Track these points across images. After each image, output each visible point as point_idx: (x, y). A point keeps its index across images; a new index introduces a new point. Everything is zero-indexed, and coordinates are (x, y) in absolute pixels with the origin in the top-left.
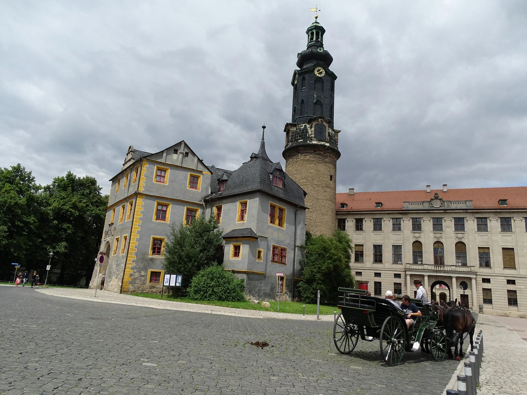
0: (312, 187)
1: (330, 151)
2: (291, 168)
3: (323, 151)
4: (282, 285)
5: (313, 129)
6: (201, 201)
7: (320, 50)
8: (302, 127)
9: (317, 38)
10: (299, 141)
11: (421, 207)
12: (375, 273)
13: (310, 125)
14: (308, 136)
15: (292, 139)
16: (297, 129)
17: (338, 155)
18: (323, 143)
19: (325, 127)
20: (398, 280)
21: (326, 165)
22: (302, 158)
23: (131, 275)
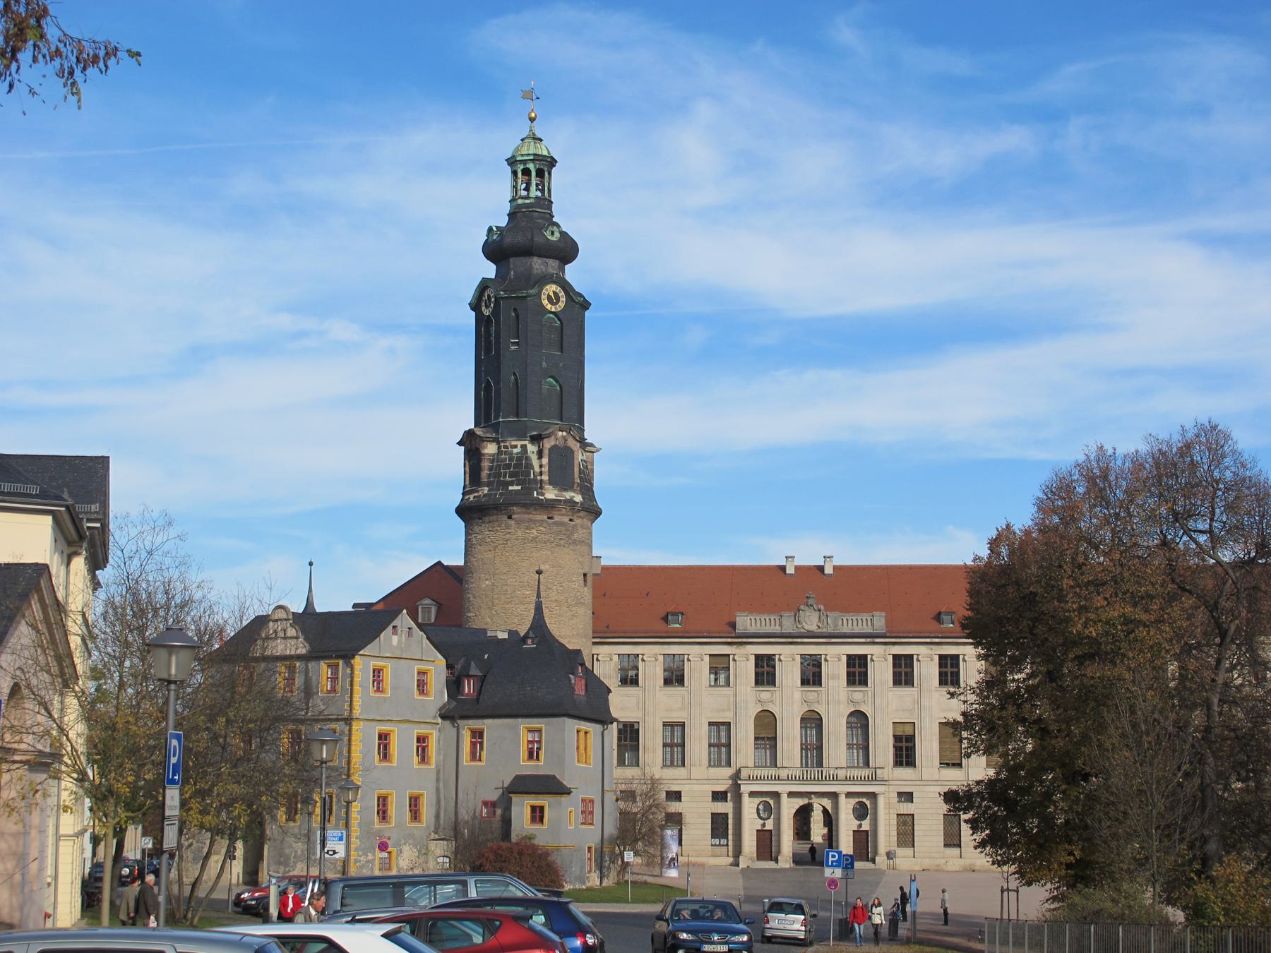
1: (582, 514)
2: (490, 555)
5: (545, 461)
8: (515, 451)
10: (511, 488)
11: (778, 628)
14: (532, 476)
15: (489, 476)
16: (500, 452)
17: (595, 513)
18: (568, 495)
20: (721, 807)
21: (574, 551)
22: (520, 533)
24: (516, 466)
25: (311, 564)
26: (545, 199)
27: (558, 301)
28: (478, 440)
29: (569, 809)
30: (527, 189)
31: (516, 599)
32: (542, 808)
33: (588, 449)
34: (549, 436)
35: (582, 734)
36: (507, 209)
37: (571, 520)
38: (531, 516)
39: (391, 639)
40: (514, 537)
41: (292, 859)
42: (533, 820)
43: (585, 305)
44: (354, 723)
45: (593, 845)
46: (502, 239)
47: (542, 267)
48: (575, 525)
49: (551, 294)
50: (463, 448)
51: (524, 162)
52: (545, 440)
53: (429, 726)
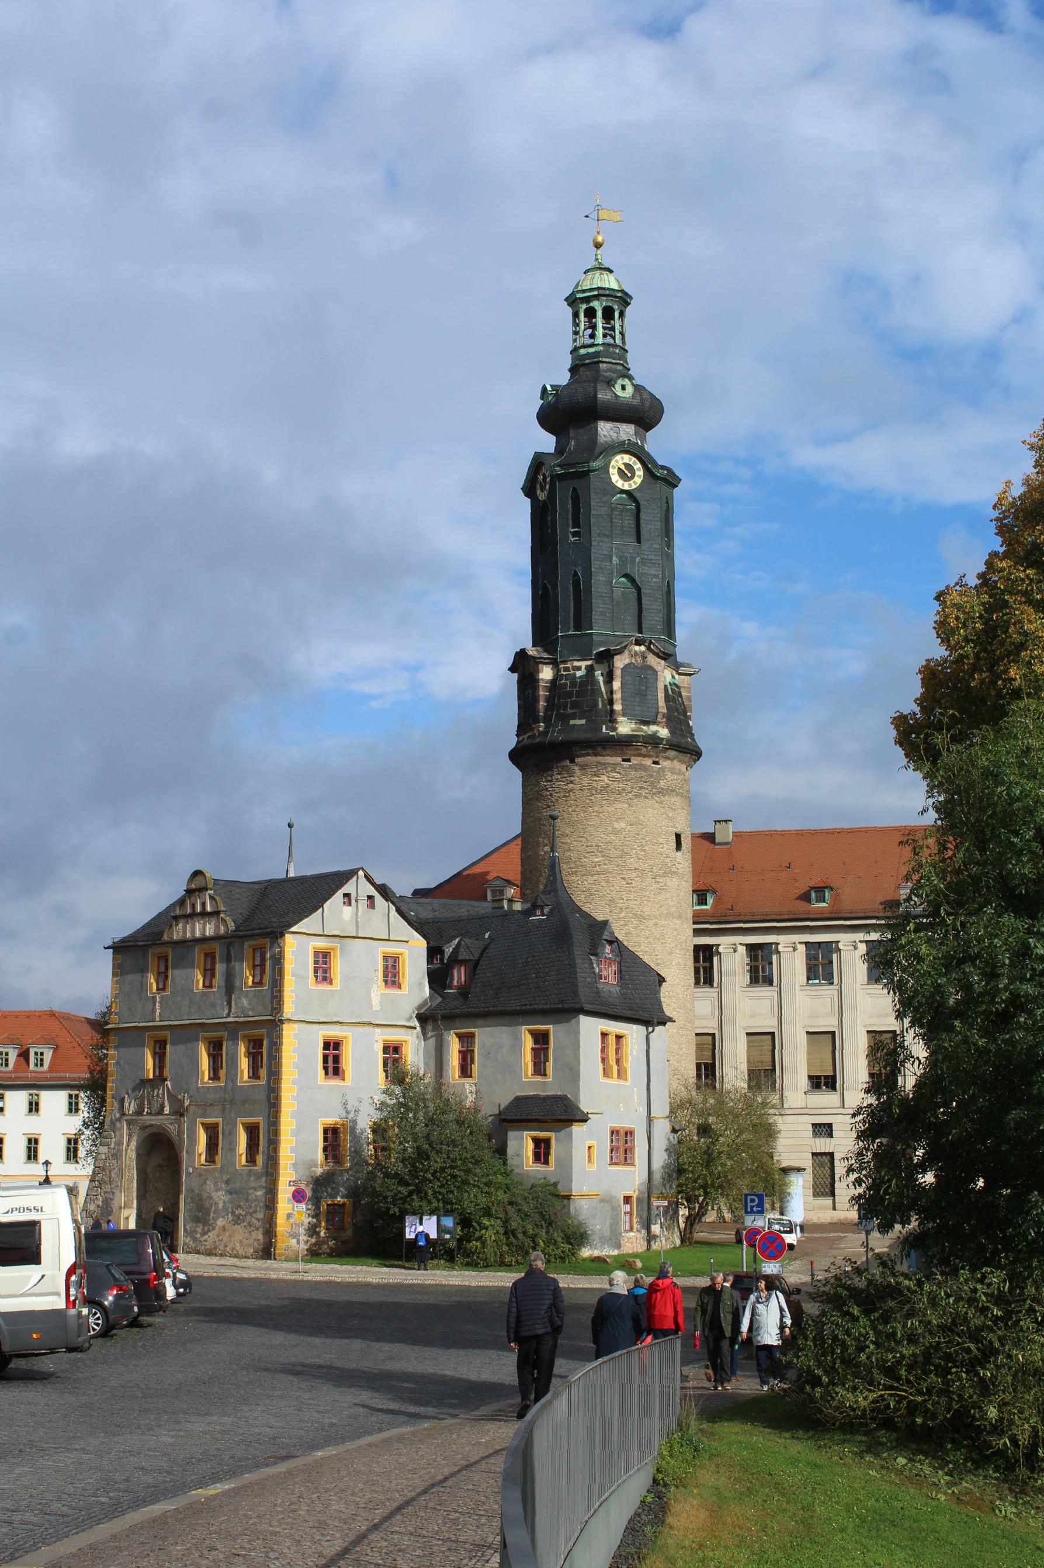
0: (624, 879)
1: (672, 753)
3: (650, 756)
4: (631, 1213)
6: (411, 1017)
7: (623, 388)
8: (579, 674)
9: (609, 330)
10: (572, 722)
12: (815, 1126)
13: (606, 665)
15: (547, 708)
19: (655, 672)
21: (661, 803)
22: (585, 781)
23: (289, 1216)
24: (578, 694)
25: (290, 826)
26: (616, 346)
27: (633, 475)
28: (532, 663)
29: (588, 1143)
30: (592, 336)
31: (581, 869)
32: (547, 1142)
33: (682, 670)
34: (620, 652)
35: (612, 1040)
36: (568, 361)
37: (655, 763)
38: (600, 759)
39: (342, 911)
40: (578, 787)
41: (212, 1215)
42: (537, 1157)
43: (671, 481)
44: (285, 1026)
45: (629, 1193)
46: (557, 399)
47: (612, 433)
48: (663, 769)
49: (623, 467)
50: (516, 675)
51: (587, 300)
52: (617, 658)
53: (403, 1030)
